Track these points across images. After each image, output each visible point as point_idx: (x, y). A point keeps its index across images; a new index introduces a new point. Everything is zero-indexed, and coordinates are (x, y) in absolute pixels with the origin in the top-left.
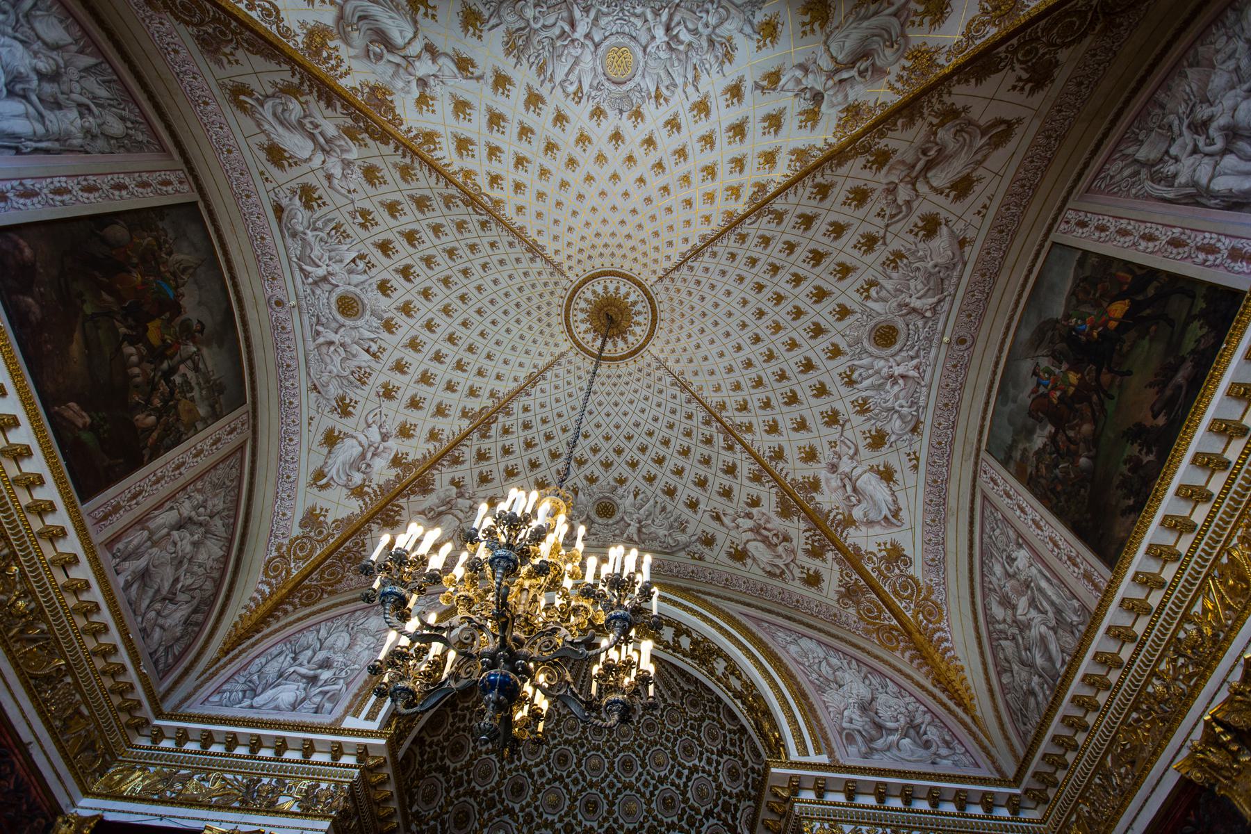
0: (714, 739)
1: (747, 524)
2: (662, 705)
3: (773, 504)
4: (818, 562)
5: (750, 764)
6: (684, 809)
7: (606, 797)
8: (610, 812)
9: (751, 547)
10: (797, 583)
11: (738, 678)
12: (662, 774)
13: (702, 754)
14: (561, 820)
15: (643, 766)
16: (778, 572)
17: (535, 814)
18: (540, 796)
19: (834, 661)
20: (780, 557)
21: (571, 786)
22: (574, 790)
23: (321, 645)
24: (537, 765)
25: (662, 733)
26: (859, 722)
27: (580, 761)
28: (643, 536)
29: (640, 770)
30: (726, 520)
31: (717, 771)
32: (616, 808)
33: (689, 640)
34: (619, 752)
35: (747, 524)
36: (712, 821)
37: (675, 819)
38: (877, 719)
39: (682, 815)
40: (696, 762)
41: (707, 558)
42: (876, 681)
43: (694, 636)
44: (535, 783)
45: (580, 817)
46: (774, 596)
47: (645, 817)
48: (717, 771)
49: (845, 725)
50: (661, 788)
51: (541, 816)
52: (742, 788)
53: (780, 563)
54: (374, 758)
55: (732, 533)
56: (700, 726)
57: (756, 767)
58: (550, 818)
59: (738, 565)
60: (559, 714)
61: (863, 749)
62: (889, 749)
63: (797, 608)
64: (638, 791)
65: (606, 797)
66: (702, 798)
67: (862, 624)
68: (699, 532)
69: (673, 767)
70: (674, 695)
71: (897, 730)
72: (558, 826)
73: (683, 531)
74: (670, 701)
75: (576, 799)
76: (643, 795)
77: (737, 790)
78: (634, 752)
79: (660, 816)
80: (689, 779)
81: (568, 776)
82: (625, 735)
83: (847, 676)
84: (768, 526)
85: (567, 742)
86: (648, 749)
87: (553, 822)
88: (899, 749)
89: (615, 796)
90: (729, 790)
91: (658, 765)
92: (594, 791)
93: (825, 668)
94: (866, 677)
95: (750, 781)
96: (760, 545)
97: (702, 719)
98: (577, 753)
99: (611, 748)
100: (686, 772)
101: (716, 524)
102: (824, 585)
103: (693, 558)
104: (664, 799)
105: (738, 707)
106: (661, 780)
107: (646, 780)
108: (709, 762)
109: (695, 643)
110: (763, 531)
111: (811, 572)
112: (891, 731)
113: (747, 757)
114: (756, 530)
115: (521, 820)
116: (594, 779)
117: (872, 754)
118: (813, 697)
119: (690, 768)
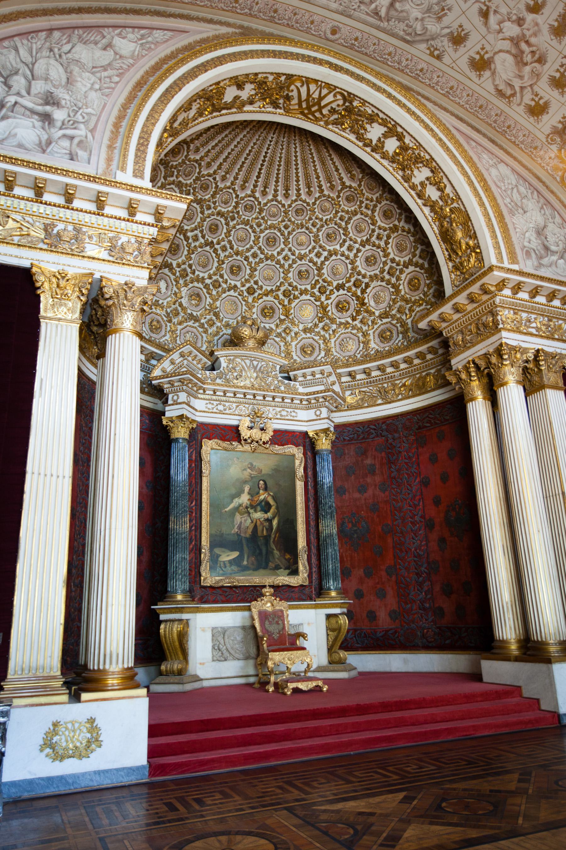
0: (360, 231)
1: (511, 29)
2: (317, 195)
3: (555, 16)
4: (556, 93)
5: (392, 256)
6: (318, 281)
7: (250, 264)
8: (251, 276)
9: (498, 59)
10: (521, 109)
11: (439, 189)
12: (303, 252)
13: (345, 241)
14: (210, 278)
15: (286, 243)
16: (509, 92)
17: (189, 270)
18: (193, 256)
19: (522, 189)
20: (521, 77)
21: (220, 252)
22: (222, 255)
23: (32, 71)
24: (192, 231)
25: (310, 219)
26: (535, 243)
27: (229, 232)
28: (393, 13)
29: (282, 246)
30: (493, 19)
31: (356, 256)
32: (257, 273)
33: (398, 144)
34: (266, 229)
35: (511, 29)
36: (341, 292)
37: (309, 287)
38: (546, 243)
39: (315, 284)
40: (338, 247)
41: (446, 59)
42: (548, 211)
43: (407, 140)
44: (189, 245)
45: (226, 277)
46: (489, 116)
47: (281, 283)
48: (356, 256)
49: (526, 244)
50: (299, 262)
51: (194, 273)
52: (377, 272)
53: (517, 84)
54: (169, 219)
55: (490, 37)
56: (350, 219)
57: (397, 259)
58: (201, 275)
59: (473, 75)
60: (217, 187)
61: (536, 263)
62: (550, 266)
63: (503, 133)
64: (278, 262)
65: (250, 264)
66: (335, 274)
67: (556, 161)
68: (455, 25)
69: (314, 248)
70: (332, 187)
71: (557, 252)
72: (208, 281)
73: (439, 19)
74: (326, 193)
75: (223, 263)
76: (282, 266)
77: (372, 273)
78: (280, 230)
79: (295, 284)
80: (326, 259)
81: (218, 243)
82: (274, 216)
83: (530, 204)
84: (533, 40)
85: (219, 213)
86: (293, 230)
87: (203, 278)
88: (556, 267)
89: (257, 264)
90: (363, 272)
91: (300, 244)
92: (239, 258)
93: (516, 196)
94: (542, 208)
95: (387, 268)
96: (510, 59)
97: (355, 213)
98: (227, 224)
99: (259, 225)
100: (325, 254)
101: (478, 21)
102: (545, 117)
103: (432, 54)
104: (300, 272)
105: (424, 216)
106: (301, 258)
107: (286, 255)
108: (350, 249)
109: (404, 148)
110: (523, 46)
111: (541, 102)
112: (554, 253)
113: (390, 250)
114: (515, 41)
115: (178, 274)
116: (240, 249)
117: (540, 267)
118: (508, 219)
119: (330, 251)
